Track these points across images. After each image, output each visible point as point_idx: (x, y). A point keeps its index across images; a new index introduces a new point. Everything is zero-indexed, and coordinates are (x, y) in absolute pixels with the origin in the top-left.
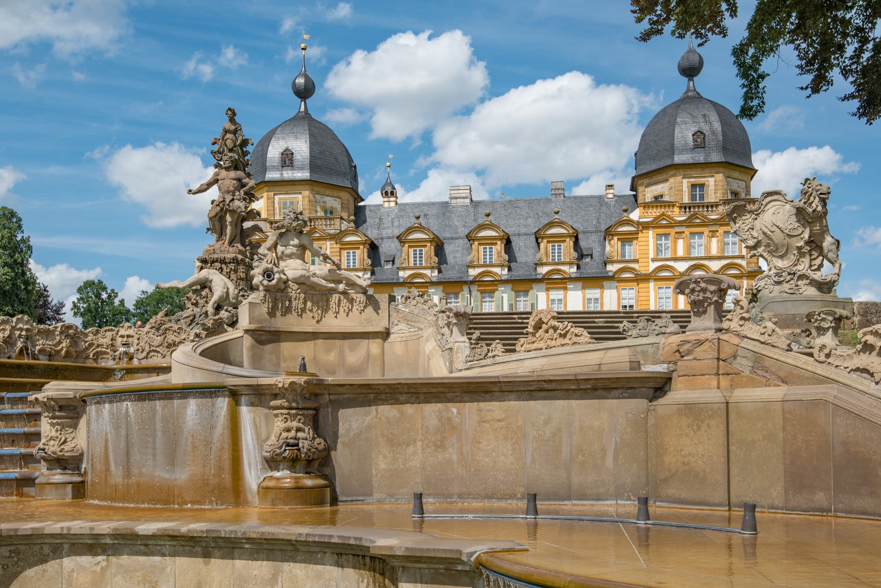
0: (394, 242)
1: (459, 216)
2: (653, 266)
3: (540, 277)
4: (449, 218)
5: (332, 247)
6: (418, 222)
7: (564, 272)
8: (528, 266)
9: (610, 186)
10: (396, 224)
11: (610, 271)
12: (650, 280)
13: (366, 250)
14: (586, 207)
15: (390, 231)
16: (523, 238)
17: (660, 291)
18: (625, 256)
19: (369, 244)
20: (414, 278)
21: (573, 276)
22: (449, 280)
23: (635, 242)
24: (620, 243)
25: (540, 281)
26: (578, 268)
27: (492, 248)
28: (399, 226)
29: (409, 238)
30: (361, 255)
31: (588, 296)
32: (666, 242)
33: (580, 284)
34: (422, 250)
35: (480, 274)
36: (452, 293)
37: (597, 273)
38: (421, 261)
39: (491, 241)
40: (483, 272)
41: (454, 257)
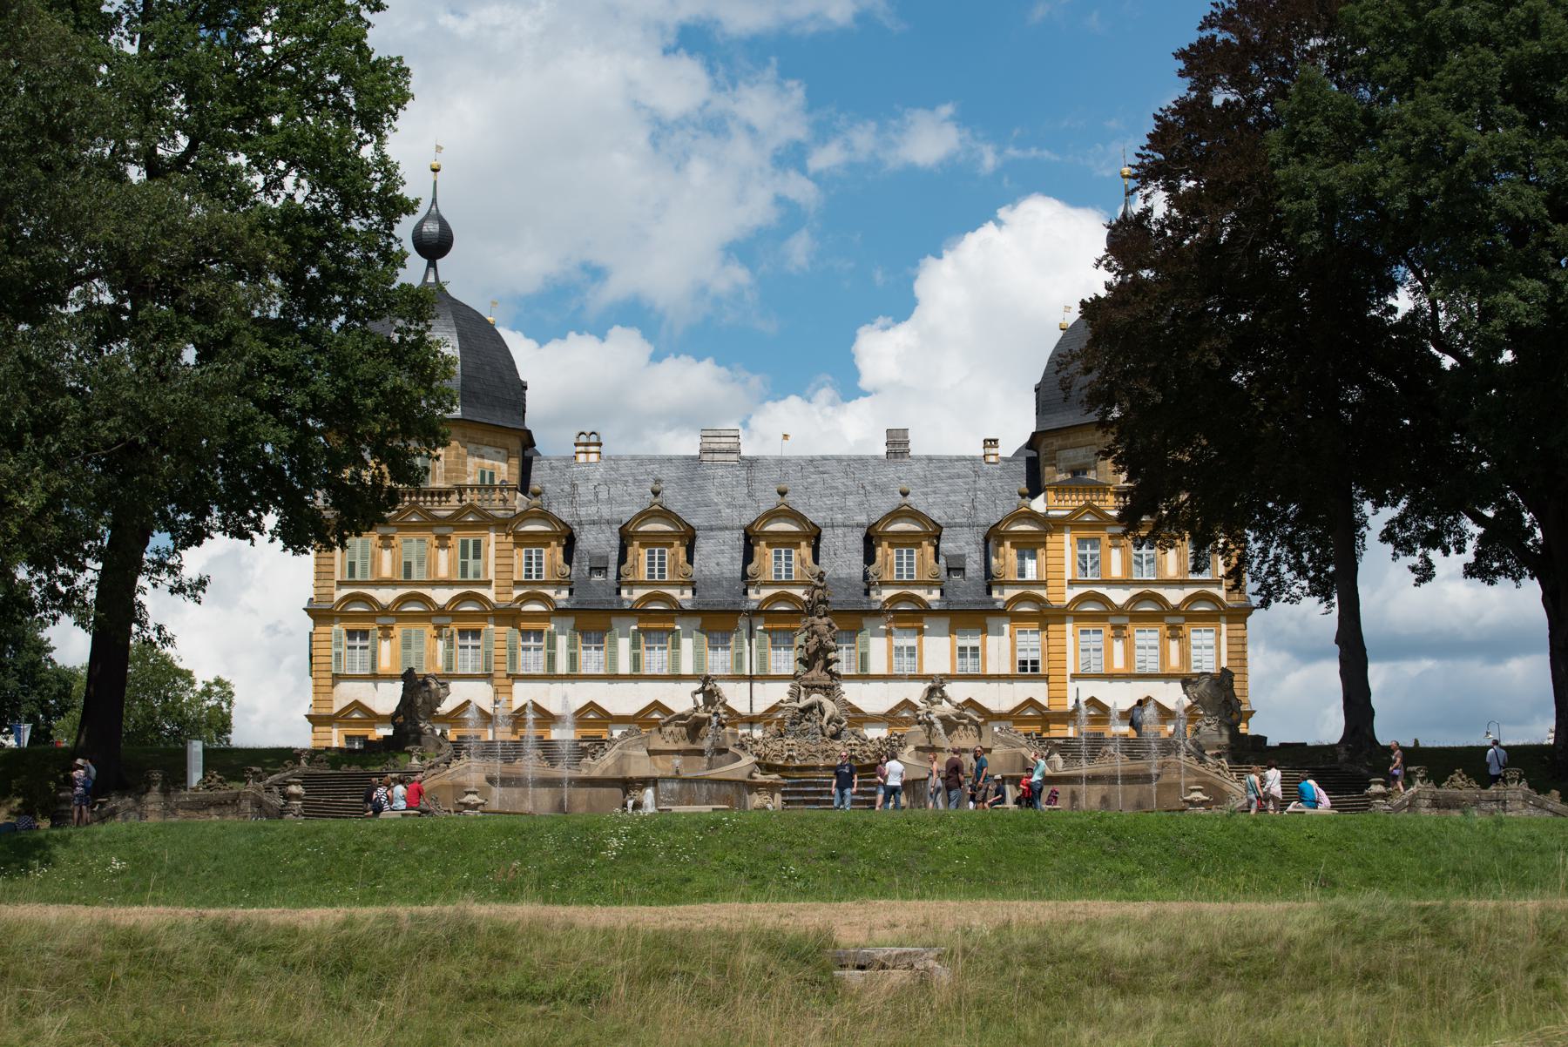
0: (603, 532)
1: (722, 485)
2: (1071, 594)
3: (878, 606)
4: (701, 488)
5: (499, 540)
6: (657, 500)
7: (919, 600)
8: (856, 586)
9: (991, 443)
10: (603, 495)
11: (997, 600)
12: (1068, 619)
13: (560, 549)
14: (950, 478)
15: (594, 509)
16: (839, 531)
17: (1086, 637)
18: (1024, 576)
19: (567, 538)
20: (651, 601)
21: (935, 606)
22: (715, 608)
23: (1040, 551)
24: (1014, 552)
25: (877, 613)
26: (942, 594)
27: (790, 552)
28: (610, 501)
29: (641, 529)
30: (552, 555)
31: (961, 642)
32: (1094, 552)
33: (945, 622)
34: (664, 552)
35: (768, 600)
36: (717, 631)
37: (976, 603)
38: (662, 570)
39: (789, 541)
40: (776, 595)
41: (718, 564)
